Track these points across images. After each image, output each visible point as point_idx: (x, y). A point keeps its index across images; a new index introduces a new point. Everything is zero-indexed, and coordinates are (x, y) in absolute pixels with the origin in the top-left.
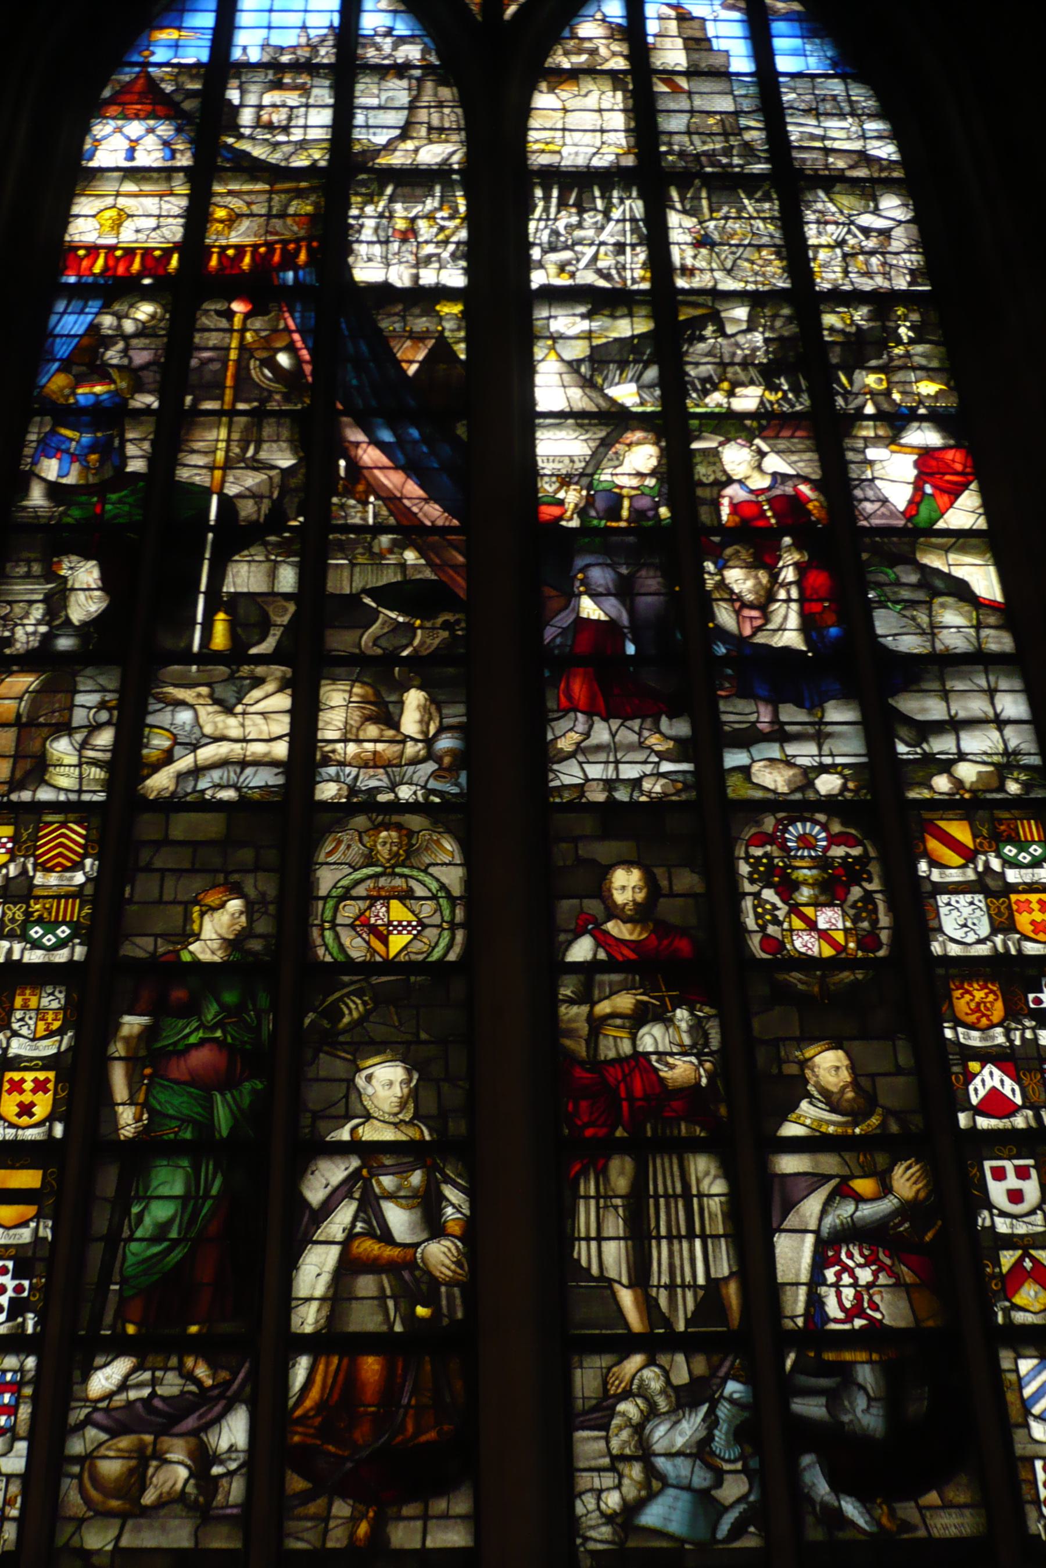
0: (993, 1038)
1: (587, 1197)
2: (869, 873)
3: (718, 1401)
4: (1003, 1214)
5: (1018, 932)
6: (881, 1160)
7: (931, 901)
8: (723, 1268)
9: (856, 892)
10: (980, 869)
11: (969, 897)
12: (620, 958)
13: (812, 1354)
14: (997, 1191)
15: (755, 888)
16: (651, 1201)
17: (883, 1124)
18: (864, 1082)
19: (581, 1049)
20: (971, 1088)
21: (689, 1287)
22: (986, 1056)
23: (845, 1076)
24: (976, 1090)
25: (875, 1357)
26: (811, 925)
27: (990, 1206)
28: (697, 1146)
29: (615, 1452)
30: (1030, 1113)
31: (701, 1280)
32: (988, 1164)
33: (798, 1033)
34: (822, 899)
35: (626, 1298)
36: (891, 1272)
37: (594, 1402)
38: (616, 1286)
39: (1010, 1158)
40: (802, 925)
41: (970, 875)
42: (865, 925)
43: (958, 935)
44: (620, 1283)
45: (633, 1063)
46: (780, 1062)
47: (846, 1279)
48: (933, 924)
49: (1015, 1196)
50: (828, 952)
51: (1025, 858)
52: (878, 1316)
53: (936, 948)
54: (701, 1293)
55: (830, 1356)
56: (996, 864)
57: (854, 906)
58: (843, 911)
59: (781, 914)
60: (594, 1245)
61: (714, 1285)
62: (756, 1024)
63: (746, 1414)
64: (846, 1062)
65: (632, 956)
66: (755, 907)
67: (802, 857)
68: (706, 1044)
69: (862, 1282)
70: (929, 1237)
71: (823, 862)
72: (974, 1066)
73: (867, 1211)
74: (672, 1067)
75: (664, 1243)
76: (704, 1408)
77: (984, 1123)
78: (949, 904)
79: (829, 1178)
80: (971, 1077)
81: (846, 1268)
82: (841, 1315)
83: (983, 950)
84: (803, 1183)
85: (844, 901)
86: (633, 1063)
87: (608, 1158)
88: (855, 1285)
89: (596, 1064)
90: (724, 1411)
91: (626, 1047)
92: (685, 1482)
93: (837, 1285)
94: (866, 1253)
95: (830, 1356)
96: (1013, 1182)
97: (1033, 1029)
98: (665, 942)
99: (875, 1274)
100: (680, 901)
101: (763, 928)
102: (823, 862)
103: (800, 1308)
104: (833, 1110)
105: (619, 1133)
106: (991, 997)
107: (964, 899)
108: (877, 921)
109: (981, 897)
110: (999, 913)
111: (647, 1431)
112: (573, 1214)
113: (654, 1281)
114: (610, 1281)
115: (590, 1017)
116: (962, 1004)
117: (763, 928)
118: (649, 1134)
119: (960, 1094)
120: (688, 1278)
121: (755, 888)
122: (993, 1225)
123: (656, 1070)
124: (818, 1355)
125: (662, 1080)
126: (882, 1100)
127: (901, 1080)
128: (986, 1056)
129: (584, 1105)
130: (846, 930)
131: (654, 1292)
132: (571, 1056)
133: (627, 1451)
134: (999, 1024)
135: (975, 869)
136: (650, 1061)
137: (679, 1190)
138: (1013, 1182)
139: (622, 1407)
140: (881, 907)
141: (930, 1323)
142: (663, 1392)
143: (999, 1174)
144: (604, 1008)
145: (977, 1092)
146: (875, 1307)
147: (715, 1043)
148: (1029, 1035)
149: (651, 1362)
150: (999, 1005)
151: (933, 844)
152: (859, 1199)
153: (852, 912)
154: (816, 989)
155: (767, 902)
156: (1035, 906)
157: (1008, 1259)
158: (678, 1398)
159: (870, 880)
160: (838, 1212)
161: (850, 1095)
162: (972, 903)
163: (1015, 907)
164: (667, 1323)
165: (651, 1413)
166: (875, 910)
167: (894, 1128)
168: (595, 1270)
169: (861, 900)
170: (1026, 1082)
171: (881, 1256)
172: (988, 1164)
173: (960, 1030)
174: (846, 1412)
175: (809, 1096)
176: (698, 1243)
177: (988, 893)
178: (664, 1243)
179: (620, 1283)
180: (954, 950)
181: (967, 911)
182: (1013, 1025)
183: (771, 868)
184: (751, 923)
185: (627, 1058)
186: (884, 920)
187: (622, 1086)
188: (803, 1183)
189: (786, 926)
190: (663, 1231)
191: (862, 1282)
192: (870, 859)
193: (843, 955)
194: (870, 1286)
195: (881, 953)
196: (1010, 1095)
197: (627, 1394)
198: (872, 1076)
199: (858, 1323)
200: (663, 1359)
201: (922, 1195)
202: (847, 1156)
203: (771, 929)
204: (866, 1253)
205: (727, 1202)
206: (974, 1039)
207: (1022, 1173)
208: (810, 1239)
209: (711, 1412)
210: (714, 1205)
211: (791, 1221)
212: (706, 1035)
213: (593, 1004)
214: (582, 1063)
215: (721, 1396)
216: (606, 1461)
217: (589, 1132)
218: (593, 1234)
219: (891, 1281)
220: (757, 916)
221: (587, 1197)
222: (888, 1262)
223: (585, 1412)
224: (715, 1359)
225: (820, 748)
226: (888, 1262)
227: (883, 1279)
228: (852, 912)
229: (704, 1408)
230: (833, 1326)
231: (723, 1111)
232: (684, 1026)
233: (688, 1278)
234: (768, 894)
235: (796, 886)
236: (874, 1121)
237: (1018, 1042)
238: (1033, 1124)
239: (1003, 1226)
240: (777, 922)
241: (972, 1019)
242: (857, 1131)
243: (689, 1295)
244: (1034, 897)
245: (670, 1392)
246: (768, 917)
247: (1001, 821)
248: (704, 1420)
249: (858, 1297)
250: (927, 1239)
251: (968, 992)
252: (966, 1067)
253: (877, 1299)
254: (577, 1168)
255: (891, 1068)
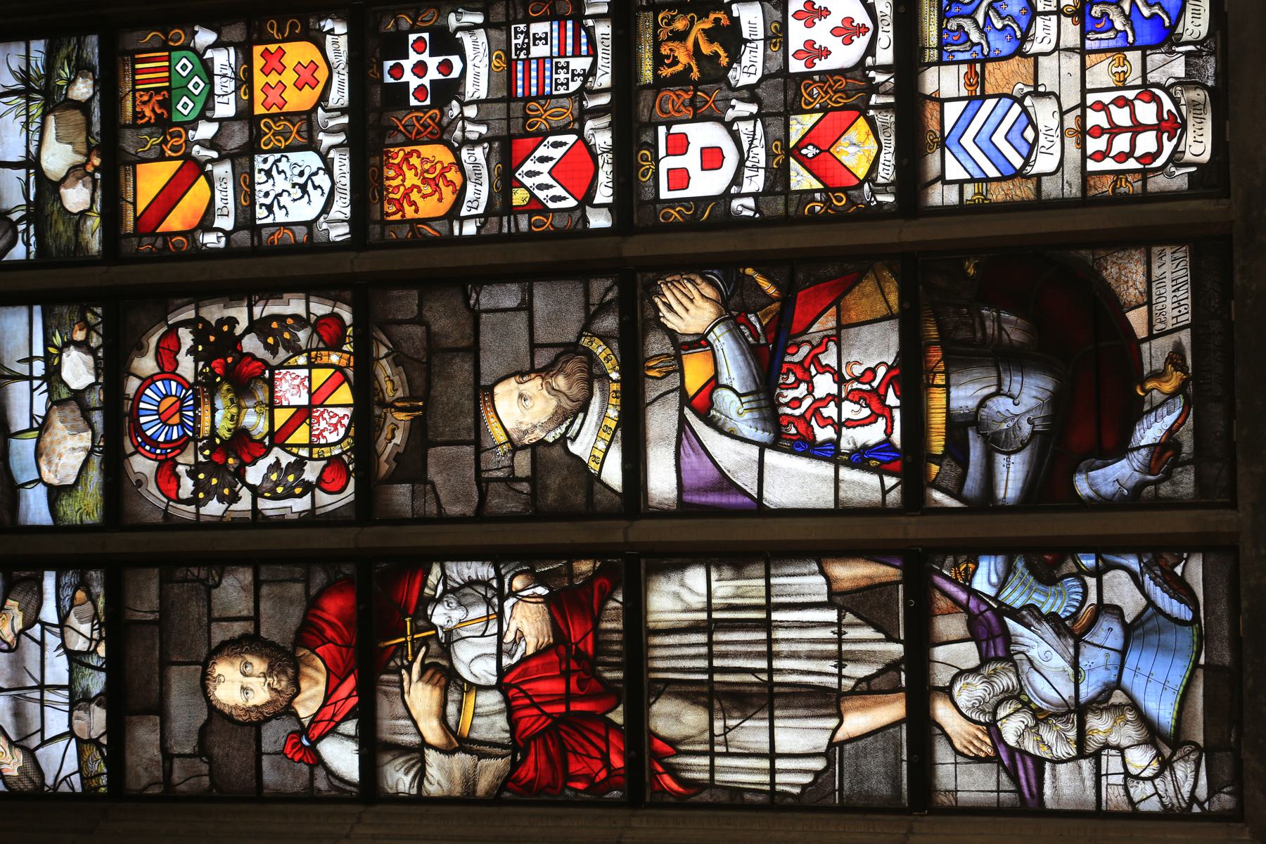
0: (476, 165)
1: (712, 769)
2: (221, 322)
3: (1001, 604)
4: (737, 179)
5: (314, 109)
6: (656, 345)
7: (265, 232)
8: (810, 584)
9: (251, 344)
10: (215, 155)
11: (260, 177)
12: (354, 701)
13: (935, 469)
14: (706, 184)
15: (246, 494)
16: (717, 678)
17: (605, 338)
18: (543, 358)
19: (491, 770)
20: (551, 205)
21: (840, 633)
22: (505, 180)
23: (533, 386)
24: (555, 199)
25: (940, 380)
26: (303, 414)
27: (727, 196)
28: (636, 609)
29: (1073, 753)
30: (590, 124)
31: (831, 616)
32: (665, 194)
33: (470, 450)
34: (262, 395)
35: (858, 721)
36: (822, 346)
37: (1004, 777)
38: (840, 735)
39: (657, 161)
40: (304, 429)
41: (223, 171)
42: (303, 335)
43: (318, 200)
44: (835, 730)
45: (513, 692)
46: (511, 479)
47: (830, 411)
48: (301, 233)
49: (711, 158)
50: (344, 394)
51: (197, 85)
52: (881, 371)
53: (339, 233)
54: (849, 617)
55: (938, 444)
56: (206, 130)
57: (273, 350)
58: (281, 366)
59: (286, 459)
60: (780, 764)
61: (837, 598)
62: (454, 510)
63: (1020, 565)
64: (512, 382)
65: (350, 683)
66: (276, 497)
67: (196, 419)
68: (486, 584)
69: (834, 389)
70: (771, 290)
71: (204, 388)
72: (519, 197)
73: (734, 369)
74: (520, 637)
75: (777, 664)
76: (1010, 623)
77: (604, 194)
78: (270, 208)
79: (683, 421)
80: (535, 207)
81: (815, 411)
82: (881, 423)
83: (342, 165)
84: (691, 460)
85: (265, 363)
86: (513, 692)
87: (654, 735)
88: (838, 400)
89: (517, 744)
90: (1015, 597)
91: (491, 700)
92: (1114, 657)
93: (839, 425)
94: (792, 379)
95: (938, 444)
96: (691, 160)
97: (463, 104)
98: (329, 633)
99: (824, 369)
100: (265, 606)
101: (308, 488)
102: (204, 388)
103: (872, 480)
104: (584, 408)
105: (617, 717)
106: (414, 160)
107: (262, 186)
108: (295, 317)
109: (259, 159)
110: (285, 134)
111: (1044, 706)
112: (736, 791)
113: (832, 682)
114: (831, 744)
115: (447, 751)
116: (430, 207)
117: (308, 488)
118: (619, 675)
119: (560, 222)
120: (827, 633)
121: (246, 494)
122: (754, 195)
123: (524, 659)
124: (938, 459)
125: (539, 653)
126: (571, 338)
127: (540, 305)
128: (505, 180)
129: (575, 767)
130: (310, 366)
131: (848, 684)
132: (506, 781)
133: (1072, 734)
134: (456, 152)
135: (212, 161)
136: (512, 667)
137: (702, 638)
138: (691, 160)
139: (1011, 739)
140: (274, 309)
141: (893, 299)
142: (989, 680)
143: (680, 178)
144: (432, 731)
145: (560, 198)
146: (873, 371)
147: (484, 571)
148: (471, 112)
149: (948, 692)
150: (426, 150)
151: (175, 221)
152: (714, 383)
153: (282, 354)
154: (401, 416)
155: (266, 477)
156: (273, 79)
157: (801, 179)
158: (997, 659)
159: (233, 322)
160: (733, 415)
161: (561, 382)
162: (268, 174)
163: (275, 110)
164: (892, 666)
165: (1017, 696)
166: (281, 318)
167: (609, 323)
168: (819, 764)
169: (263, 337)
170: (544, 126)
171: (796, 359)
172: (665, 194)
173: (464, 212)
174: (1017, 427)
175: (563, 440)
176: (776, 616)
177: (252, 148)
178: (777, 664)
179: (835, 730)
180: (342, 208)
181: (281, 183)
182: (458, 134)
183: (213, 467)
184: (300, 505)
185: (507, 700)
186: (295, 306)
187: (548, 709)
188: (691, 460)
189: (304, 453)
190: (762, 664)
191: (834, 389)
192: (199, 319)
193: (350, 373)
194: (840, 380)
195: (347, 316)
196: (562, 150)
197: (993, 729)
198: (534, 346)
199: (892, 400)
200: (942, 676)
201: (709, 291)
202: (651, 395)
203: (311, 473)
204: (792, 379)
205: (718, 567)
206: (478, 195)
207: (679, 146)
208: (771, 457)
209: (1015, 614)
210: (724, 589)
211: (747, 481)
212: (471, 583)
213: (424, 744)
214: (514, 765)
215: (995, 599)
216: (1086, 765)
217: (617, 762)
218: (765, 764)
219: (833, 347)
220: (289, 494)
221: (712, 769)
222: (805, 350)
223: (1019, 790)
224: (943, 603)
225: (21, 377)
226: (805, 350)
227: (830, 359)
228: (282, 354)
229: (1010, 623)
230: (896, 437)
231: (585, 566)
232: (458, 614)
233: (827, 633)
234: (254, 475)
235: (241, 434)
236: (599, 349)
237: (483, 129)
238: (605, 121)
239: (755, 182)
240: (299, 464)
241: (449, 196)
242: (615, 376)
243: (851, 633)
244: (259, 80)
245: (988, 669)
246: (291, 478)
247: (136, 115)
248: (1028, 626)
249: (856, 397)
250: (771, 290)
251: (406, 195)
252: (521, 210)
253: (858, 371)
254: (668, 781)
255: (523, 315)
